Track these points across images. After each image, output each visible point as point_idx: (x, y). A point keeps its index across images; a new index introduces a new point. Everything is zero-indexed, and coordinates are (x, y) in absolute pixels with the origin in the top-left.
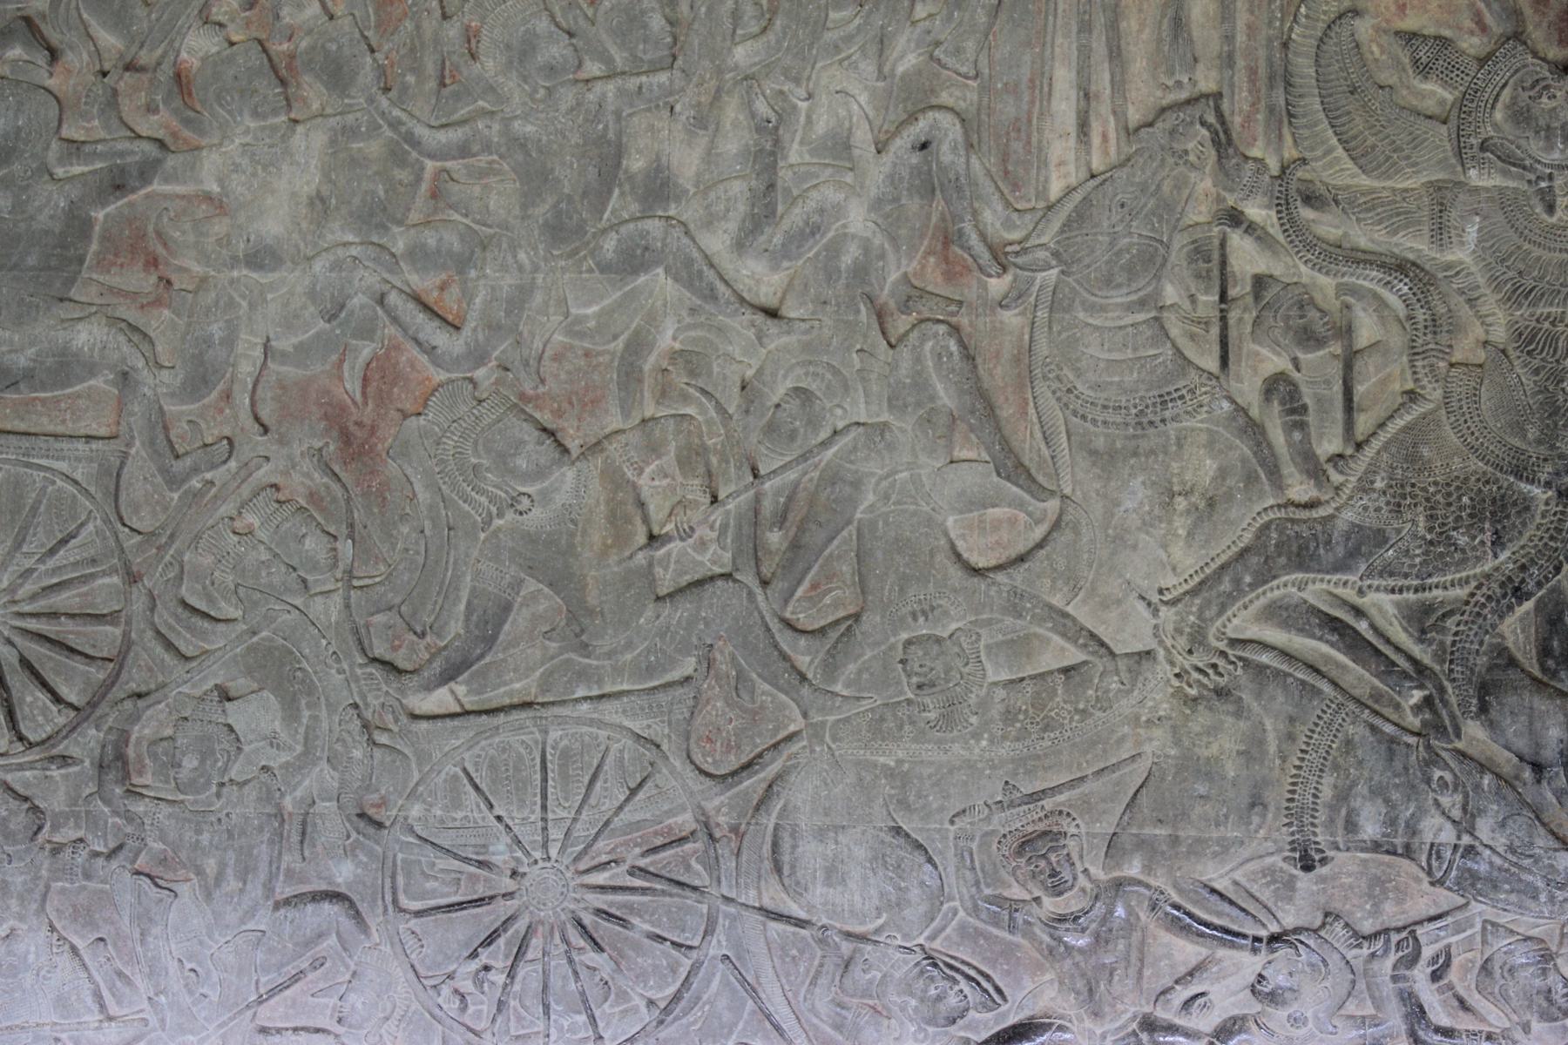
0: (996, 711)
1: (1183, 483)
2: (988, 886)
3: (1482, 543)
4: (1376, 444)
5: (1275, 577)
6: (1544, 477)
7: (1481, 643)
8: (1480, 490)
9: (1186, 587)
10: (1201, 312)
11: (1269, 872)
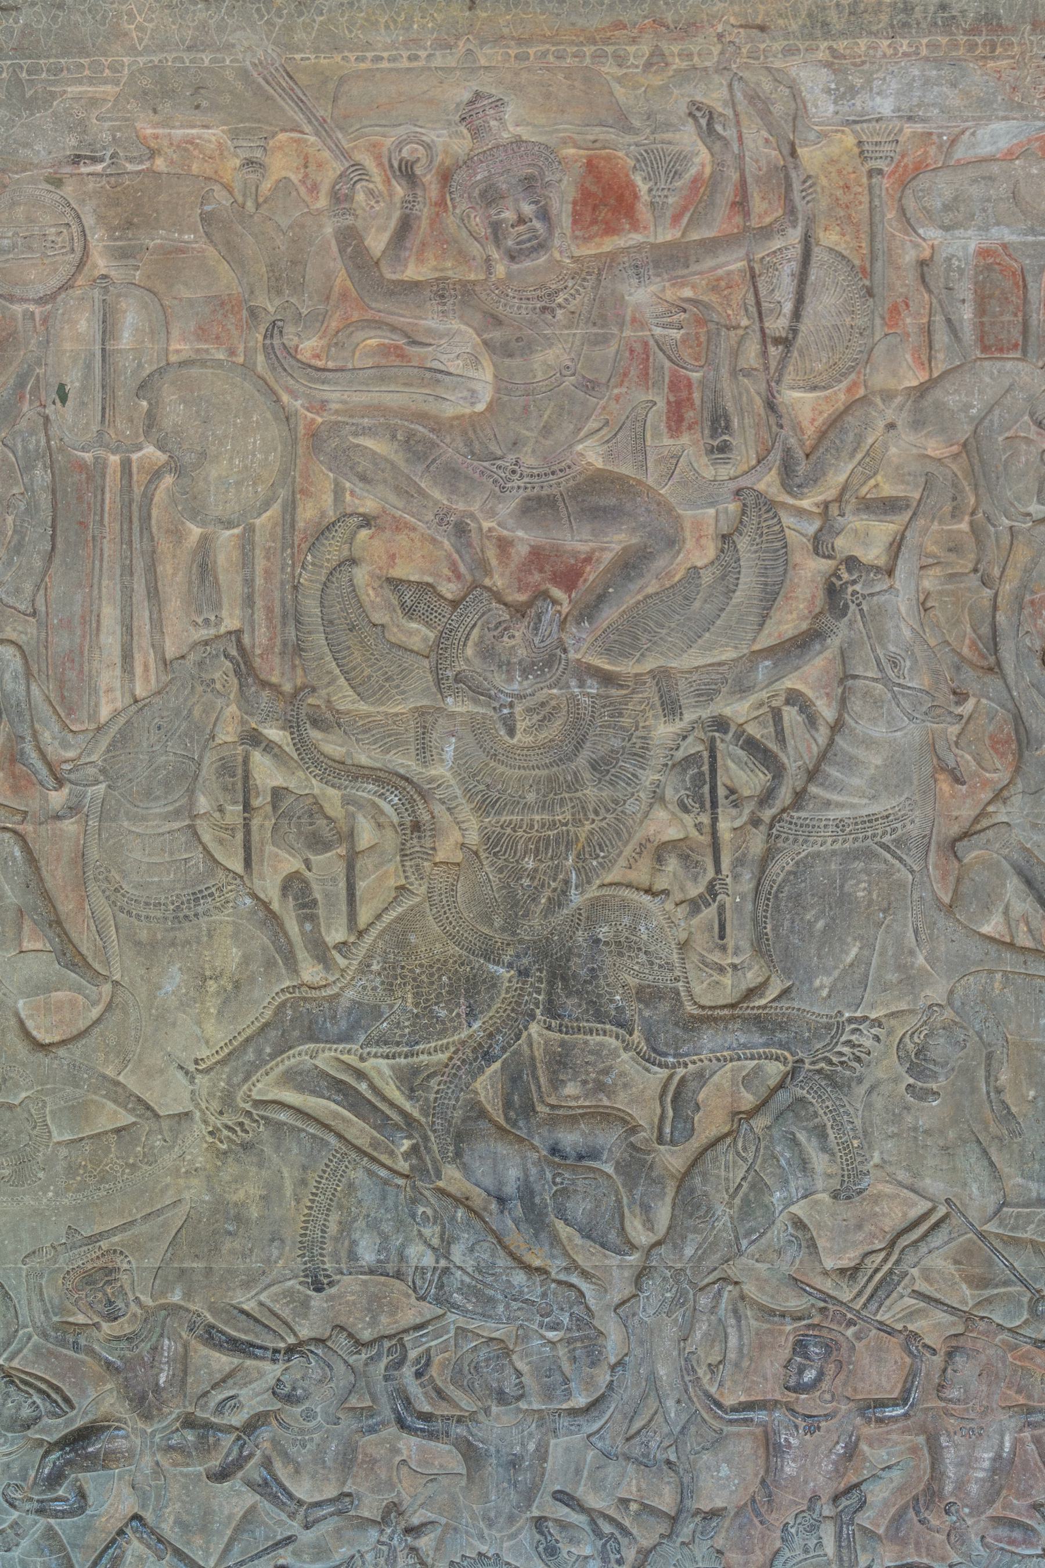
0: (60, 1168)
1: (214, 969)
2: (56, 1315)
3: (458, 1015)
4: (374, 932)
5: (290, 1048)
6: (507, 959)
7: (457, 1100)
8: (456, 971)
9: (218, 1057)
10: (229, 820)
11: (289, 1293)
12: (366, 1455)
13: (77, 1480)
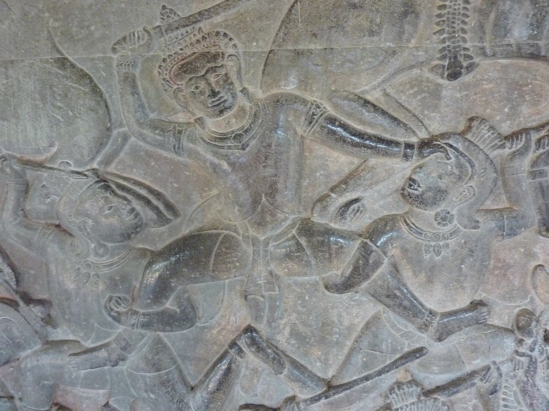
2: (153, 111)
11: (417, 83)
12: (499, 260)
13: (185, 292)
